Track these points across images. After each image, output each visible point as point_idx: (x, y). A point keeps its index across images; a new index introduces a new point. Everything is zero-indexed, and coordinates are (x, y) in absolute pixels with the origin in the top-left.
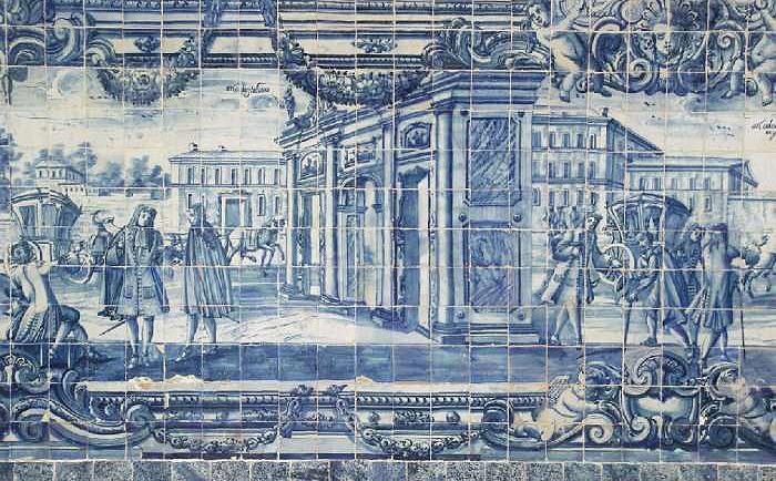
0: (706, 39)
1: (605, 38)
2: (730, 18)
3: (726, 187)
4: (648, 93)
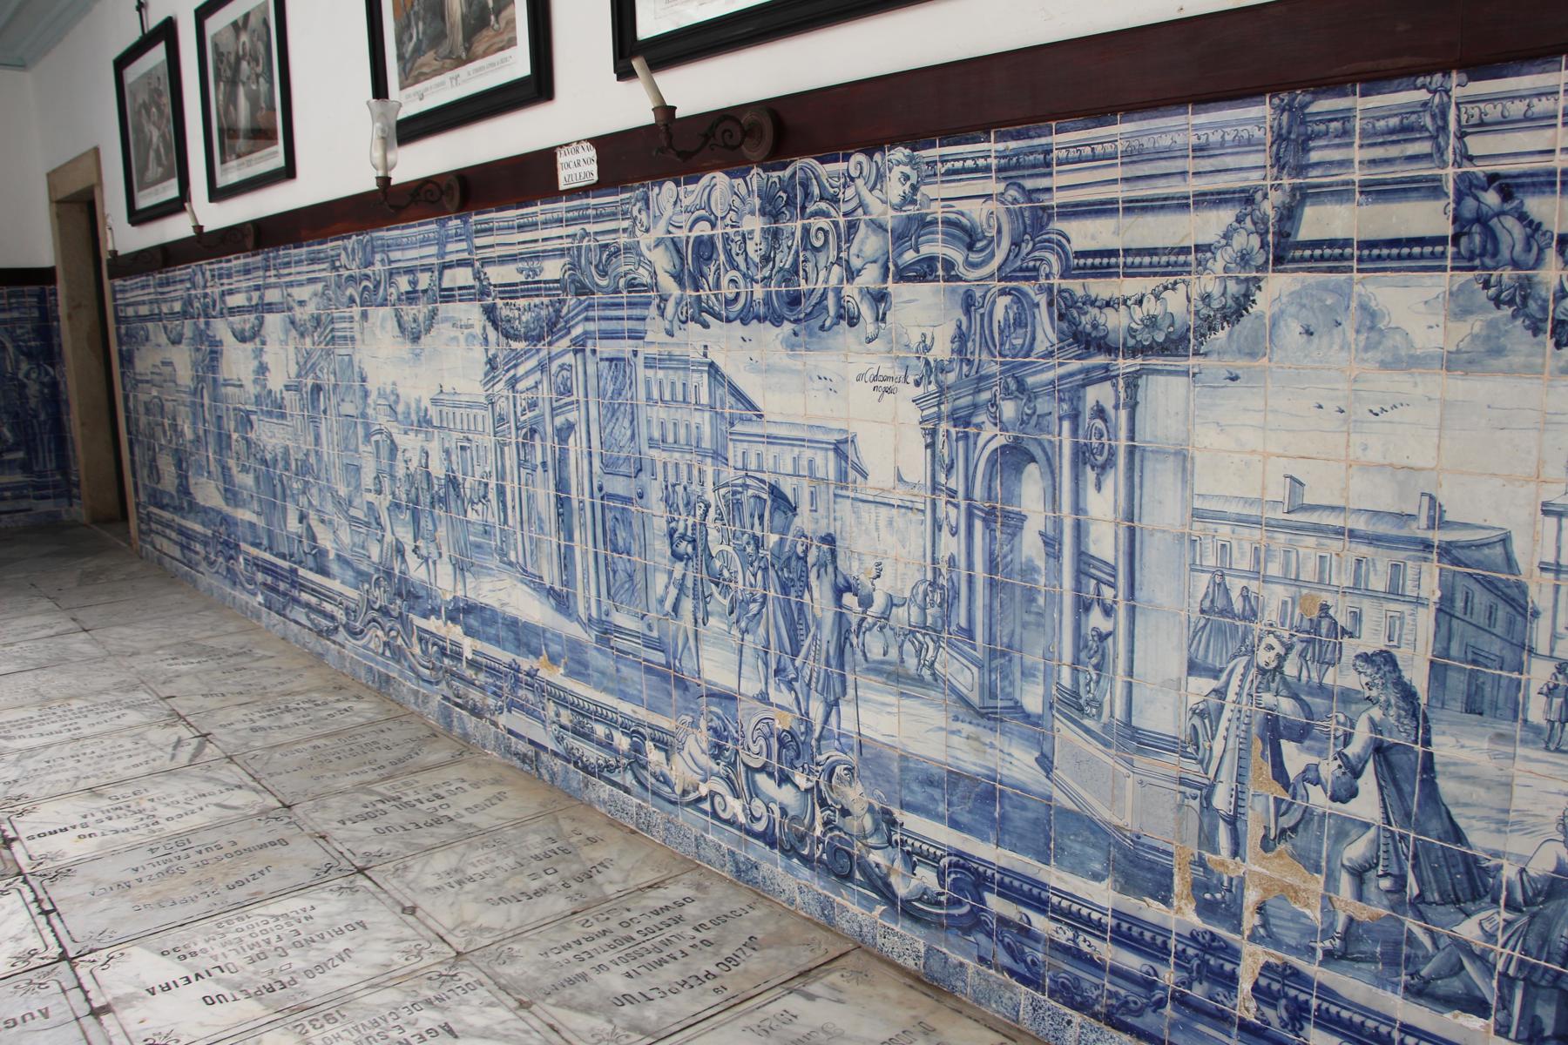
0: (798, 234)
1: (699, 241)
2: (822, 199)
3: (832, 476)
4: (744, 322)
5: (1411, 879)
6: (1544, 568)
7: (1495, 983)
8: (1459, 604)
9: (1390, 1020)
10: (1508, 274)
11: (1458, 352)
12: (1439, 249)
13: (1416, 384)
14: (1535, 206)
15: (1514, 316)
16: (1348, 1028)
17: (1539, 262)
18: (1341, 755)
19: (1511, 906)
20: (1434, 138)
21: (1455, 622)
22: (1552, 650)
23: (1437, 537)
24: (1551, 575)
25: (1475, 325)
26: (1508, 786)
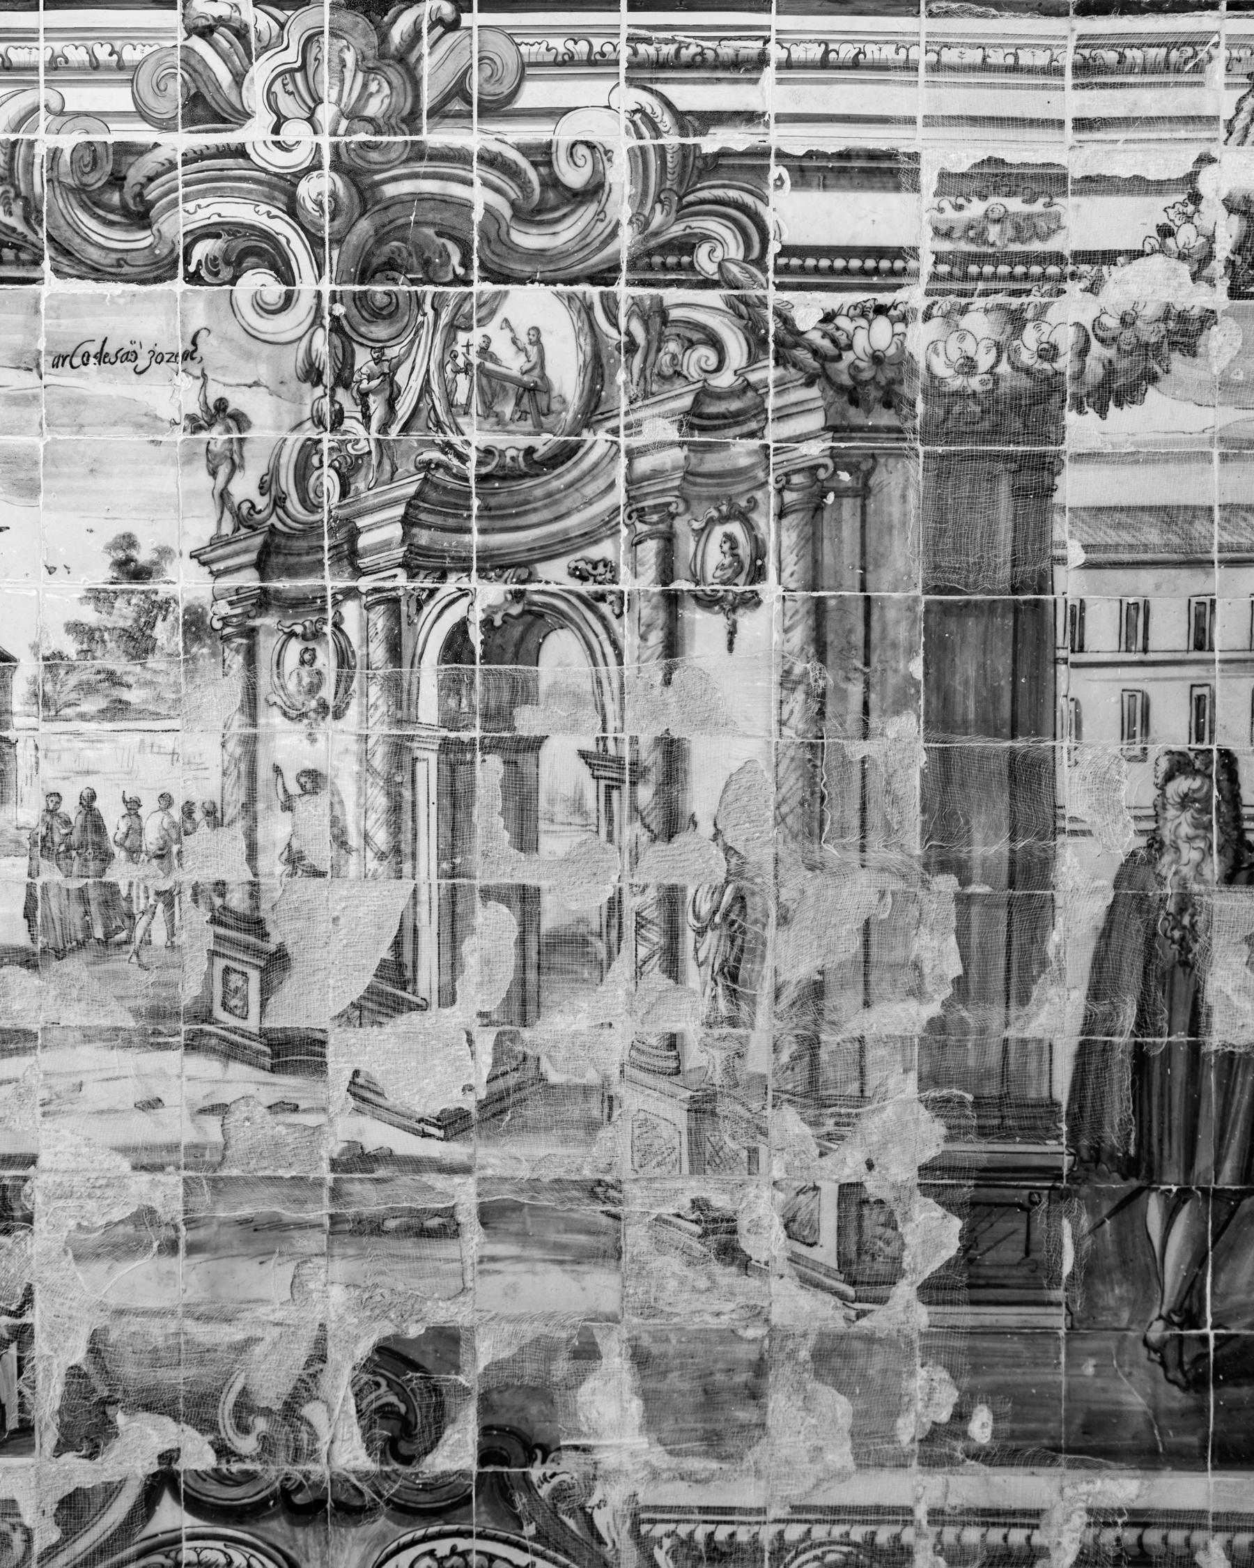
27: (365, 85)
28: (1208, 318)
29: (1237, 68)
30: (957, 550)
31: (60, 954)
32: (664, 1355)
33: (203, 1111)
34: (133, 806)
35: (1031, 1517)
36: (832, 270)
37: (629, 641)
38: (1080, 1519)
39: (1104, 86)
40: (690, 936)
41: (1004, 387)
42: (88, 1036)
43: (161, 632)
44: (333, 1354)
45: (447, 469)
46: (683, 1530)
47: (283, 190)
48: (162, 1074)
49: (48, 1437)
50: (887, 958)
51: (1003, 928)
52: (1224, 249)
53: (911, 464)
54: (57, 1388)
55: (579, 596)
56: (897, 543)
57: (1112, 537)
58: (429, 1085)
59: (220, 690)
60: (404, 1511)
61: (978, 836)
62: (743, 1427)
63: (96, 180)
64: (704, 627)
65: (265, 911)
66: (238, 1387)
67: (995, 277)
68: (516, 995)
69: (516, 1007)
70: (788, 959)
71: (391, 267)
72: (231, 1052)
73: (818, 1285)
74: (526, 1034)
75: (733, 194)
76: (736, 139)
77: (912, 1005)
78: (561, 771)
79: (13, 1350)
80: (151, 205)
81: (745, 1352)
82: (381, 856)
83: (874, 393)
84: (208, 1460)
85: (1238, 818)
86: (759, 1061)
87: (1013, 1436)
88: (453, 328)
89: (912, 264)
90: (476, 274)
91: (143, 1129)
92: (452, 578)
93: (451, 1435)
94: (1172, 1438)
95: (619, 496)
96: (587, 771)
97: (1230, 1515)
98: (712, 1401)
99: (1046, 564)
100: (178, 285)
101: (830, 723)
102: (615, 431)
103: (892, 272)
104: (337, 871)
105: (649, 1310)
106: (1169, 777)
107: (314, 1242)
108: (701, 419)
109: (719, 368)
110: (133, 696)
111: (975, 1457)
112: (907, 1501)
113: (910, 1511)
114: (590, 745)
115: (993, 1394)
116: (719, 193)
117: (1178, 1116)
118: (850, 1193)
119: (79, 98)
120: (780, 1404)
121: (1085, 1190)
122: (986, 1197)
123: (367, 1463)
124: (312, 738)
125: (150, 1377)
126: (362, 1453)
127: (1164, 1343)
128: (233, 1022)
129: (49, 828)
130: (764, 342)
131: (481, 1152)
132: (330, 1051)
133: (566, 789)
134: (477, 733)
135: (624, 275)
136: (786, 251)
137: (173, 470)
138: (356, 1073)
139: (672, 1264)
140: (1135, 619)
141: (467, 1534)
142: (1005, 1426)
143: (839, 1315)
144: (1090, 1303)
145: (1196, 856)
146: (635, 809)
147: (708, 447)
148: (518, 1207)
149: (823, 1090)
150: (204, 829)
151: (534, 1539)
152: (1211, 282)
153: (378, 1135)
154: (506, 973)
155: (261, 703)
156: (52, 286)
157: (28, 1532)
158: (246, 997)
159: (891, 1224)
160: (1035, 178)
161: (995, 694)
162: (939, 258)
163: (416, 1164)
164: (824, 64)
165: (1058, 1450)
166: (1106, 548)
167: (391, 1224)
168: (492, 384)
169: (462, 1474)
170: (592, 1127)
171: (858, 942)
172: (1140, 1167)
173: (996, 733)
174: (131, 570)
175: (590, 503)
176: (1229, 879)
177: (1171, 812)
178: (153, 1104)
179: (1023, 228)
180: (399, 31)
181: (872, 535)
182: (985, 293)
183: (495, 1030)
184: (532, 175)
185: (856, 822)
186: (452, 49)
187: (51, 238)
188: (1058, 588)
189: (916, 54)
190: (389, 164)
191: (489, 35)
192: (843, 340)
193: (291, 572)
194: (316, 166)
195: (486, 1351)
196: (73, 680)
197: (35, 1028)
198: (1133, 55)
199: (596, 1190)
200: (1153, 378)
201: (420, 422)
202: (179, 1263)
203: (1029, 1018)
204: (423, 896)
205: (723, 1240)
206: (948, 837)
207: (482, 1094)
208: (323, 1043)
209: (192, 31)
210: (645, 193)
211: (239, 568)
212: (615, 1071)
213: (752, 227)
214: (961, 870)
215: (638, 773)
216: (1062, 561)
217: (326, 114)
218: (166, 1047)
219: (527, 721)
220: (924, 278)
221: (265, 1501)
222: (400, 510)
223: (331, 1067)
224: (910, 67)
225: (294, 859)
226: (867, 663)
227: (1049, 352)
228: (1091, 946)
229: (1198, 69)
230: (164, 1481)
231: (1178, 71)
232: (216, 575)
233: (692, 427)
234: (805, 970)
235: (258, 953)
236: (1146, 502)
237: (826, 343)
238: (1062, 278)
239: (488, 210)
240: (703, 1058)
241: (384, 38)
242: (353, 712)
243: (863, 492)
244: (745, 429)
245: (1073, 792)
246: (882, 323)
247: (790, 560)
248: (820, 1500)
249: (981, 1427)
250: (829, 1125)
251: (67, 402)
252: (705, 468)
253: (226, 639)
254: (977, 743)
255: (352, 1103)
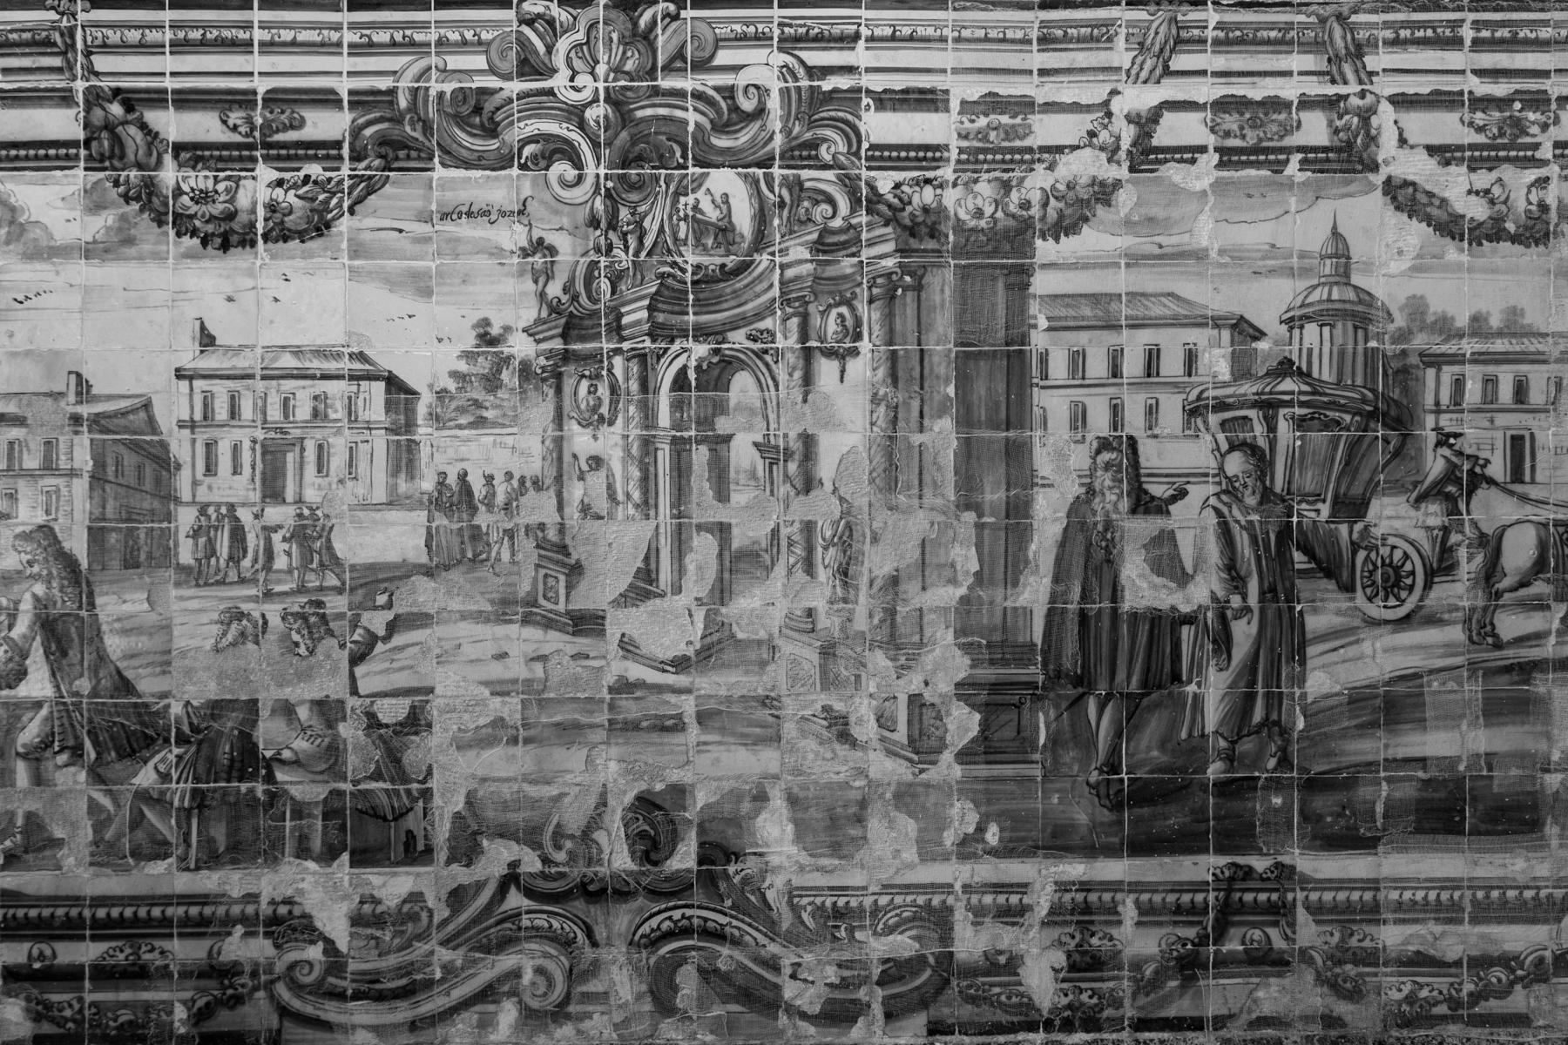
5: (88, 744)
6: (181, 425)
7: (173, 822)
8: (111, 469)
9: (76, 900)
10: (133, 174)
11: (95, 242)
12: (73, 151)
13: (58, 273)
14: (153, 117)
15: (142, 210)
16: (37, 927)
17: (159, 164)
18: (7, 639)
19: (182, 740)
20: (64, 53)
21: (108, 487)
22: (194, 496)
23: (85, 410)
24: (187, 432)
25: (108, 218)
26: (166, 628)
27: (624, 53)
28: (1117, 184)
29: (1132, 39)
30: (974, 322)
31: (447, 568)
32: (807, 798)
33: (532, 659)
34: (489, 479)
35: (1022, 888)
36: (899, 159)
37: (782, 377)
38: (1050, 888)
39: (1055, 50)
40: (820, 550)
41: (1000, 225)
42: (464, 616)
43: (505, 375)
44: (611, 802)
45: (674, 277)
46: (818, 901)
47: (575, 114)
48: (508, 637)
49: (442, 855)
50: (935, 561)
51: (1003, 542)
52: (1125, 144)
53: (946, 271)
54: (448, 826)
55: (753, 351)
56: (939, 317)
57: (1063, 312)
58: (666, 641)
59: (540, 411)
60: (654, 893)
61: (988, 489)
62: (853, 839)
63: (465, 110)
64: (826, 369)
65: (568, 541)
66: (555, 822)
67: (994, 161)
68: (718, 585)
69: (717, 595)
70: (877, 563)
71: (639, 160)
72: (548, 624)
73: (897, 755)
74: (724, 610)
75: (841, 114)
76: (843, 82)
77: (950, 589)
78: (743, 453)
79: (421, 803)
80: (498, 124)
81: (854, 795)
82: (637, 506)
83: (924, 230)
84: (537, 866)
85: (1138, 475)
86: (861, 623)
87: (1011, 841)
88: (677, 194)
89: (946, 154)
90: (690, 162)
91: (496, 671)
92: (678, 341)
93: (681, 848)
94: (1103, 839)
95: (776, 292)
96: (757, 454)
97: (1138, 883)
98: (834, 824)
99: (1025, 328)
100: (515, 171)
101: (901, 424)
102: (773, 254)
103: (934, 159)
104: (611, 516)
105: (797, 771)
106: (1098, 452)
107: (599, 736)
108: (823, 246)
109: (834, 216)
110: (489, 414)
111: (989, 853)
112: (950, 881)
113: (951, 886)
114: (759, 439)
115: (999, 817)
116: (833, 114)
117: (1105, 650)
118: (915, 701)
119: (455, 62)
120: (875, 825)
121: (1052, 695)
122: (995, 700)
123: (631, 866)
124: (595, 438)
125: (503, 817)
126: (629, 860)
127: (1098, 783)
128: (550, 606)
129: (440, 493)
130: (860, 200)
131: (698, 680)
132: (607, 622)
133: (746, 465)
134: (693, 433)
135: (777, 163)
136: (872, 147)
137: (512, 281)
138: (623, 635)
139: (811, 744)
140: (1077, 360)
141: (692, 906)
142: (1007, 834)
143: (909, 772)
144: (1056, 762)
145: (1114, 498)
146: (786, 476)
147: (828, 263)
148: (719, 712)
149: (898, 639)
150: (532, 492)
151: (731, 908)
152: (1119, 163)
153: (636, 672)
154: (711, 574)
155: (565, 418)
156: (439, 173)
157: (430, 912)
158: (557, 592)
159: (939, 717)
160: (1016, 103)
161: (997, 404)
162: (961, 151)
163: (659, 689)
164: (893, 38)
165: (1037, 847)
166: (1060, 318)
167: (645, 724)
168: (700, 227)
169: (688, 871)
170: (763, 664)
171: (918, 552)
172: (1083, 681)
173: (997, 428)
174: (487, 339)
175: (758, 296)
176: (1134, 511)
177: (1099, 473)
178: (502, 656)
179: (1010, 132)
180: (643, 22)
181: (924, 313)
182: (988, 171)
183: (705, 608)
184: (723, 104)
185: (916, 482)
186: (675, 31)
187: (439, 144)
188: (1033, 342)
189: (946, 32)
190: (639, 99)
191: (698, 23)
192: (906, 199)
193: (583, 339)
194: (596, 100)
195: (701, 798)
196: (454, 405)
197: (432, 612)
198: (1072, 32)
199: (765, 701)
200: (1086, 220)
201: (658, 250)
202: (519, 750)
203: (1018, 595)
204: (662, 530)
205: (840, 729)
206: (970, 490)
207: (698, 646)
208: (603, 618)
209: (521, 22)
210: (789, 114)
211: (552, 337)
212: (777, 631)
213: (853, 134)
214: (978, 509)
215: (788, 454)
216: (1035, 326)
217: (601, 69)
218: (511, 622)
219: (723, 425)
220: (953, 163)
221: (571, 890)
222: (646, 302)
223: (608, 631)
224: (943, 39)
225: (585, 509)
226: (922, 388)
227: (1025, 205)
228: (1055, 550)
229: (1110, 40)
230: (511, 878)
231: (1098, 41)
232: (538, 342)
233: (818, 251)
234: (887, 569)
235: (564, 565)
236: (1082, 291)
237: (896, 201)
238: (1033, 162)
239: (697, 124)
240: (827, 622)
241: (635, 24)
242: (620, 421)
243: (918, 288)
244: (849, 251)
245: (1043, 462)
246: (928, 190)
247: (876, 328)
248: (898, 881)
249: (992, 836)
250: (903, 660)
251: (449, 241)
252: (826, 275)
253: (544, 380)
254: (986, 434)
255: (621, 653)
